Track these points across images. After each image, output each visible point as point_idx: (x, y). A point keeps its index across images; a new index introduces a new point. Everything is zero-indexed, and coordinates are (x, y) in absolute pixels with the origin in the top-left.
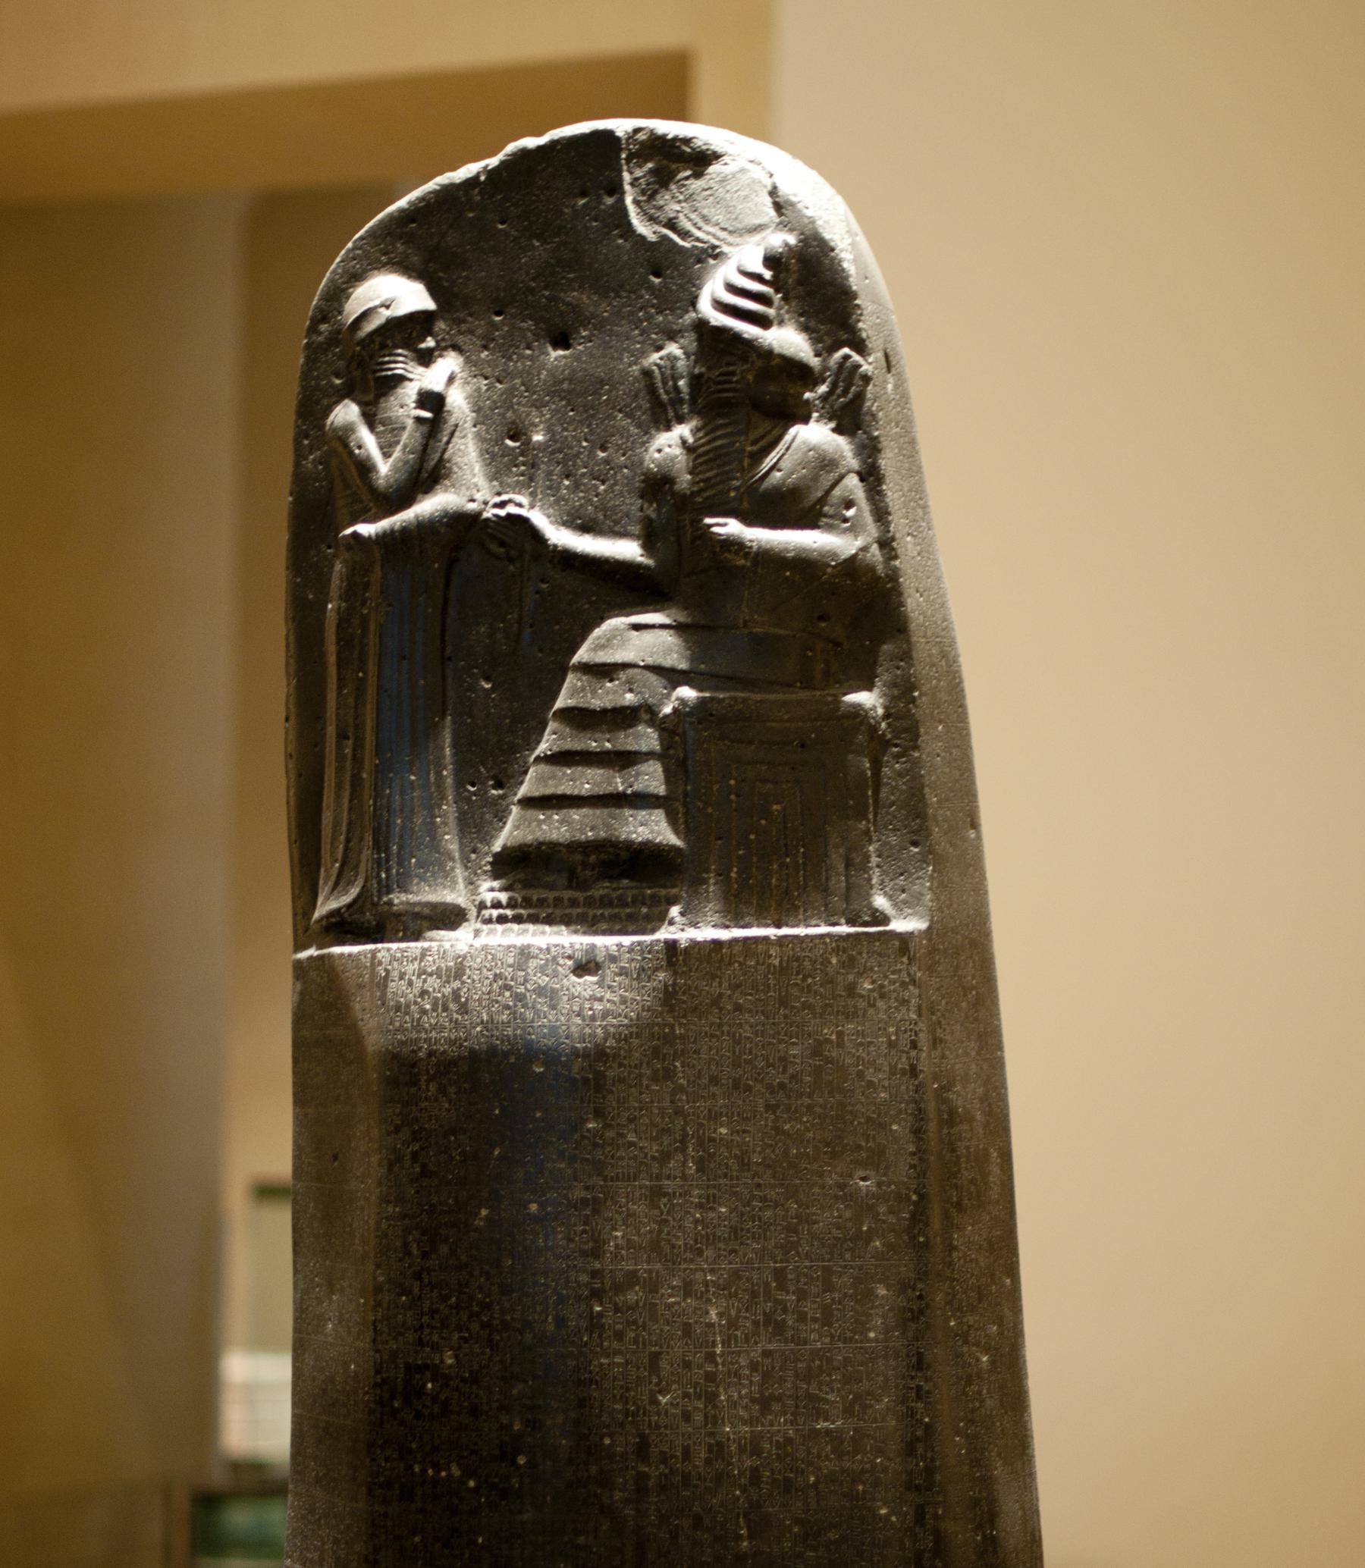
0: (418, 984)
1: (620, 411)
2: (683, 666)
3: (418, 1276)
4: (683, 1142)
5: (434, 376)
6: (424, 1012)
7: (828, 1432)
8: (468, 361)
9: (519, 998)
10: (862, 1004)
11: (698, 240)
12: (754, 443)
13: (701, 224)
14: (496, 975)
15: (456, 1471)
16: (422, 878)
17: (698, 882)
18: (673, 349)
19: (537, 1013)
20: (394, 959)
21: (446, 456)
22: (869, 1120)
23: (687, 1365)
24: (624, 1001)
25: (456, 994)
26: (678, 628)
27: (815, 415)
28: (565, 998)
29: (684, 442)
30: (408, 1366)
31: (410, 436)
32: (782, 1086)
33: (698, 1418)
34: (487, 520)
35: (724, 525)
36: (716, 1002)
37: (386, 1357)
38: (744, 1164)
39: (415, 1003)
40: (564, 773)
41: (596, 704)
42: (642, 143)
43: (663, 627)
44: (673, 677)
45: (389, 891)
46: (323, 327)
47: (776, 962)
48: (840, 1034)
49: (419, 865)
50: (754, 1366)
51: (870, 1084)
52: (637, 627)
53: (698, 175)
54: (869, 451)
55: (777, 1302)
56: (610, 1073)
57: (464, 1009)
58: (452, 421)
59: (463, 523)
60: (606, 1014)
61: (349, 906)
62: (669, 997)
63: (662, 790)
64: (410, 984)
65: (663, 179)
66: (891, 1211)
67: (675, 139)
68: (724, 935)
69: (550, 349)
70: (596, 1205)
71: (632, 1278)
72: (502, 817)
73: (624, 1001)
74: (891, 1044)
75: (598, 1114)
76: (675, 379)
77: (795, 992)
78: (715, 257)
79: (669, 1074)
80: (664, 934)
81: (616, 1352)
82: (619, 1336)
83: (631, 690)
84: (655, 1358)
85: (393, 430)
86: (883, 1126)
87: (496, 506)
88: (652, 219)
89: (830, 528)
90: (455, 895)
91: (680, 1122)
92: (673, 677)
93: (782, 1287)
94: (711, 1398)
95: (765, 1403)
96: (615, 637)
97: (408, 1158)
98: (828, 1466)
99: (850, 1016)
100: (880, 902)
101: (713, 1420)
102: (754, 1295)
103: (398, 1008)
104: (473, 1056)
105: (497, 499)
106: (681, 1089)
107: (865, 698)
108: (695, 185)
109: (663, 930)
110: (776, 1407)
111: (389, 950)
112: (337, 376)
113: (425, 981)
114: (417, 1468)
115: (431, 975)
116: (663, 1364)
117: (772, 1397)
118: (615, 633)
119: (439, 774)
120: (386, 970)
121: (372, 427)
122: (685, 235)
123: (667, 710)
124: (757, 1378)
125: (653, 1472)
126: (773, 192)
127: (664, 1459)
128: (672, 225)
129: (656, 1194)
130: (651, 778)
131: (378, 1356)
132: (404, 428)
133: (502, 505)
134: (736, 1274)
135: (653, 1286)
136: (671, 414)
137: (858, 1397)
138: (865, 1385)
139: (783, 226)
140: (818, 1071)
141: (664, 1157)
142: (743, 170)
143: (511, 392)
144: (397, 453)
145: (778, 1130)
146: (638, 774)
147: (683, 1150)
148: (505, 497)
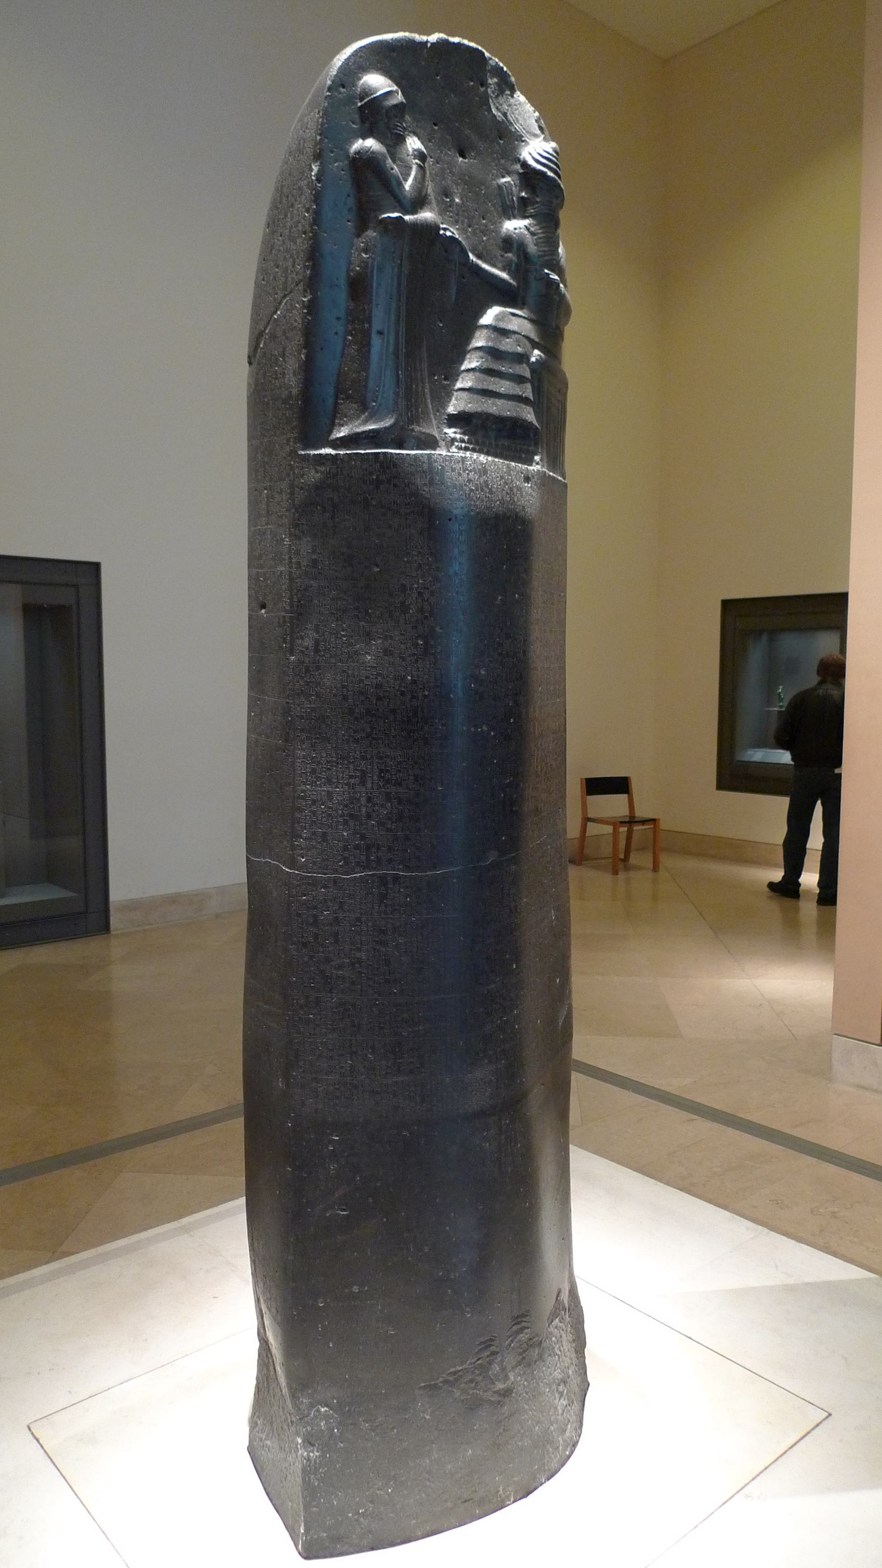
2: (537, 340)
15: (485, 728)
25: (486, 482)
26: (531, 321)
39: (466, 485)
43: (524, 318)
45: (412, 424)
46: (342, 90)
52: (514, 315)
57: (491, 492)
61: (385, 428)
63: (531, 397)
64: (460, 474)
72: (449, 396)
76: (513, 196)
78: (523, 141)
80: (535, 468)
88: (497, 108)
90: (435, 433)
92: (535, 345)
103: (455, 486)
104: (497, 516)
115: (471, 471)
121: (394, 161)
123: (533, 359)
128: (505, 114)
130: (527, 391)
131: (439, 672)
133: (445, 229)
143: (443, 170)
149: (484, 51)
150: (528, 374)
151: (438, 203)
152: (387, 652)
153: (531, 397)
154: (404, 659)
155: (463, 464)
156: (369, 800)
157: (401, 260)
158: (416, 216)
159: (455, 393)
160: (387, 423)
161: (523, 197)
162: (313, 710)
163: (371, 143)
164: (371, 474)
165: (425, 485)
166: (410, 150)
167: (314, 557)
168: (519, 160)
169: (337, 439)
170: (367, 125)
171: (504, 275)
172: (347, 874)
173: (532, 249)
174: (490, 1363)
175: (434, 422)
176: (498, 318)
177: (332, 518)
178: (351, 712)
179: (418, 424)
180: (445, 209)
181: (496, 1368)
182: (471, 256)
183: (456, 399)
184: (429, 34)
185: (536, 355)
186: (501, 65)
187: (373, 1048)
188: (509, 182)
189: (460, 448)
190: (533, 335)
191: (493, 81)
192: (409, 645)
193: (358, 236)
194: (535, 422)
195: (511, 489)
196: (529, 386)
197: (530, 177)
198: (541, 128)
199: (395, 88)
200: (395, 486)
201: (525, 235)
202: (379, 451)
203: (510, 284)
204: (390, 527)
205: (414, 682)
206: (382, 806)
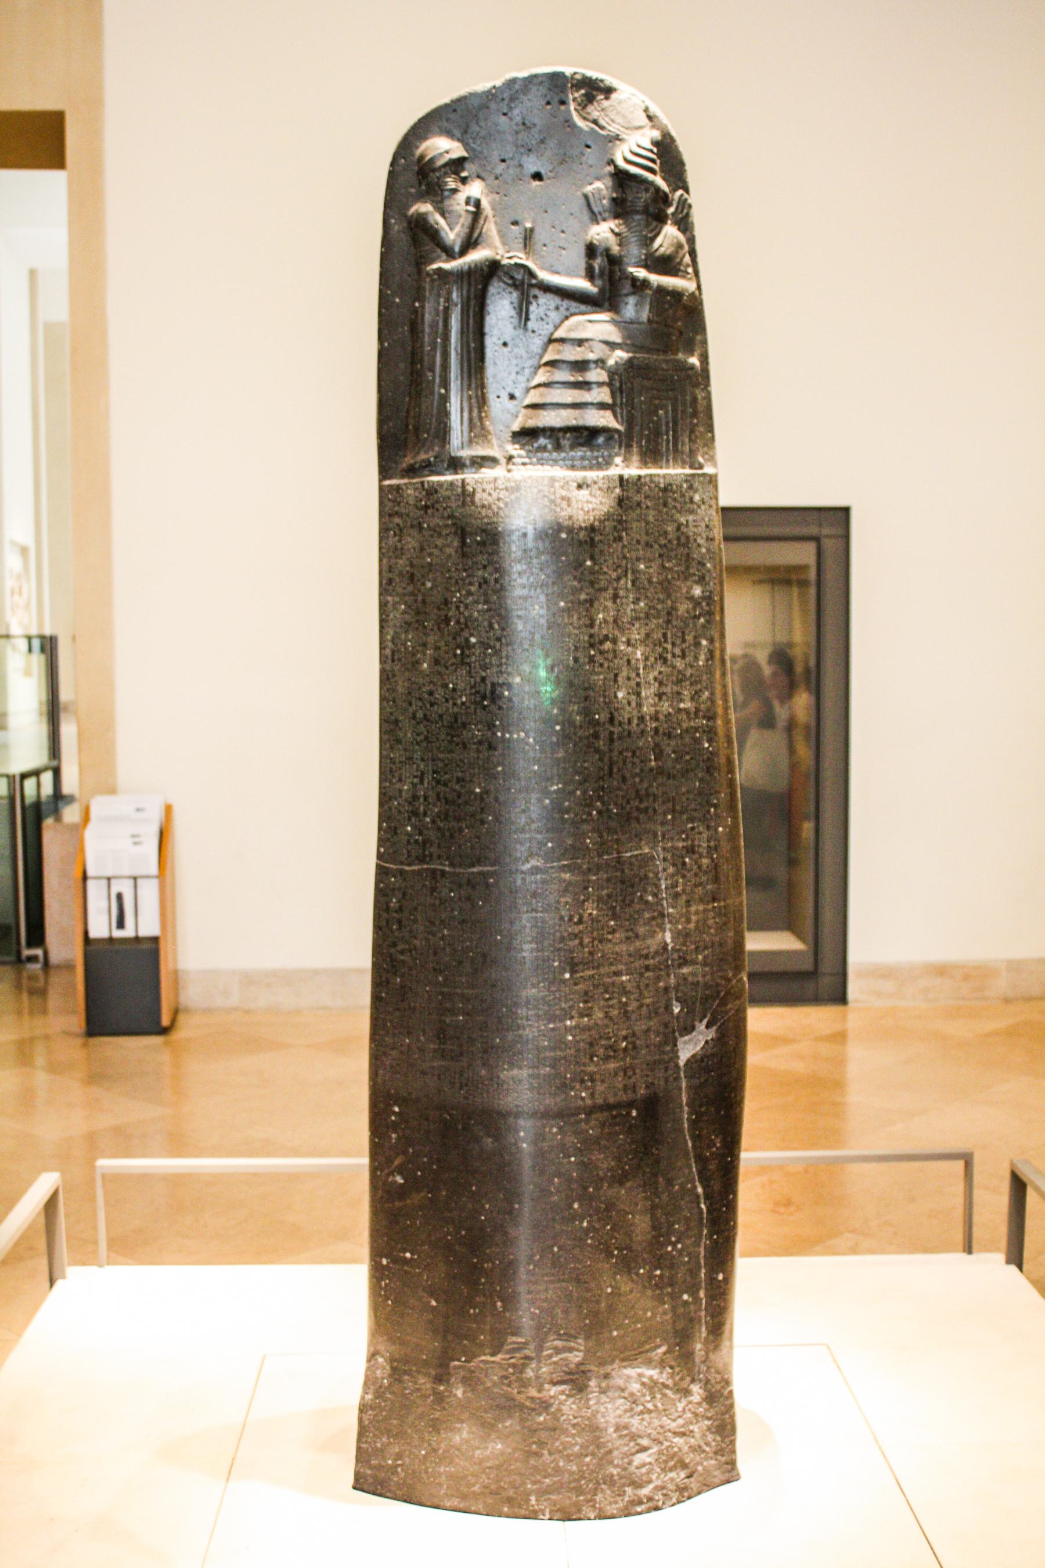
0: (495, 495)
2: (619, 340)
3: (499, 639)
4: (626, 572)
5: (475, 189)
6: (499, 508)
7: (685, 709)
8: (487, 185)
9: (553, 502)
10: (695, 507)
12: (652, 231)
16: (477, 443)
17: (629, 446)
18: (599, 185)
19: (562, 509)
20: (477, 482)
21: (484, 230)
22: (699, 563)
23: (629, 679)
24: (601, 503)
26: (613, 322)
27: (669, 222)
29: (612, 231)
30: (493, 685)
31: (465, 220)
32: (665, 545)
33: (634, 704)
36: (639, 504)
37: (478, 679)
38: (650, 581)
42: (578, 80)
44: (612, 345)
47: (662, 486)
48: (687, 521)
49: (475, 437)
50: (655, 679)
51: (699, 546)
52: (590, 321)
53: (607, 98)
54: (691, 241)
55: (664, 648)
56: (597, 539)
58: (485, 214)
59: (493, 268)
60: (593, 510)
62: (620, 501)
63: (610, 401)
64: (490, 494)
65: (590, 99)
66: (708, 604)
68: (644, 472)
70: (591, 602)
71: (606, 638)
73: (601, 503)
74: (707, 526)
75: (592, 558)
77: (670, 500)
78: (620, 140)
79: (620, 538)
81: (601, 673)
82: (601, 665)
84: (616, 675)
86: (704, 565)
88: (585, 119)
89: (684, 277)
91: (624, 562)
93: (666, 641)
94: (638, 694)
95: (660, 696)
97: (492, 583)
98: (685, 725)
99: (692, 512)
100: (701, 459)
101: (639, 705)
102: (655, 645)
103: (483, 506)
105: (508, 255)
106: (624, 546)
107: (694, 361)
108: (606, 104)
110: (664, 698)
114: (499, 734)
116: (620, 679)
117: (664, 694)
118: (579, 324)
122: (602, 128)
123: (611, 362)
124: (657, 685)
125: (616, 730)
126: (646, 110)
127: (620, 724)
128: (595, 122)
129: (615, 597)
130: (603, 395)
133: (510, 258)
134: (648, 635)
135: (614, 641)
136: (599, 217)
137: (696, 692)
138: (699, 686)
139: (653, 127)
140: (678, 539)
141: (619, 579)
142: (629, 98)
144: (458, 228)
145: (663, 567)
147: (626, 575)
148: (511, 254)
152: (437, 662)
154: (447, 668)
156: (426, 798)
162: (391, 714)
164: (421, 500)
167: (390, 575)
170: (423, 187)
172: (409, 865)
173: (615, 249)
174: (524, 1366)
175: (494, 441)
177: (400, 541)
178: (414, 717)
181: (530, 1373)
185: (620, 355)
187: (424, 1031)
192: (451, 655)
196: (606, 390)
200: (438, 510)
204: (436, 546)
205: (454, 690)
206: (434, 805)
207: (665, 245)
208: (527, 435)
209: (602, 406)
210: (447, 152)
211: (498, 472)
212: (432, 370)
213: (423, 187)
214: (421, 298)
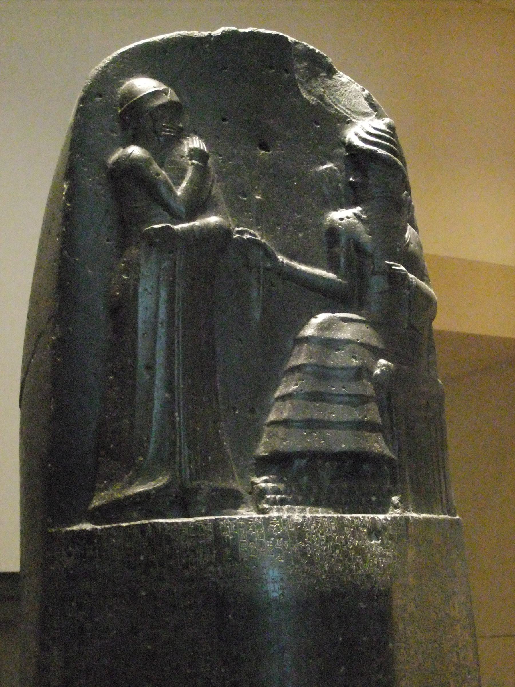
1: (305, 193)
2: (381, 346)
11: (336, 110)
13: (336, 103)
14: (327, 537)
18: (329, 165)
28: (369, 555)
34: (236, 239)
35: (399, 266)
40: (315, 406)
41: (330, 363)
46: (98, 99)
57: (311, 562)
60: (389, 565)
61: (158, 490)
63: (379, 420)
64: (261, 544)
67: (319, 53)
69: (258, 149)
78: (348, 122)
83: (354, 357)
85: (180, 169)
87: (238, 232)
88: (309, 92)
90: (237, 485)
92: (377, 353)
96: (333, 324)
105: (237, 229)
108: (330, 82)
109: (390, 512)
111: (231, 519)
112: (112, 131)
113: (274, 542)
119: (217, 399)
120: (232, 534)
121: (161, 166)
123: (378, 371)
128: (321, 98)
130: (373, 413)
132: (185, 170)
133: (241, 232)
146: (368, 410)
148: (241, 228)
149: (287, 36)
150: (370, 390)
151: (230, 205)
153: (379, 420)
155: (266, 529)
157: (174, 276)
158: (191, 224)
159: (266, 428)
160: (161, 481)
161: (351, 182)
163: (135, 151)
165: (211, 563)
166: (186, 150)
168: (344, 143)
169: (96, 509)
171: (331, 275)
173: (366, 238)
176: (323, 327)
179: (207, 478)
180: (238, 209)
182: (280, 258)
183: (269, 437)
184: (214, 29)
186: (312, 47)
188: (331, 168)
189: (274, 502)
190: (375, 341)
191: (302, 66)
193: (120, 256)
194: (387, 452)
195: (346, 554)
197: (357, 158)
198: (372, 106)
199: (163, 87)
201: (355, 225)
202: (146, 522)
203: (340, 283)
207: (412, 241)
208: (277, 463)
209: (372, 427)
210: (155, 94)
211: (246, 513)
212: (150, 367)
213: (130, 132)
214: (133, 268)
